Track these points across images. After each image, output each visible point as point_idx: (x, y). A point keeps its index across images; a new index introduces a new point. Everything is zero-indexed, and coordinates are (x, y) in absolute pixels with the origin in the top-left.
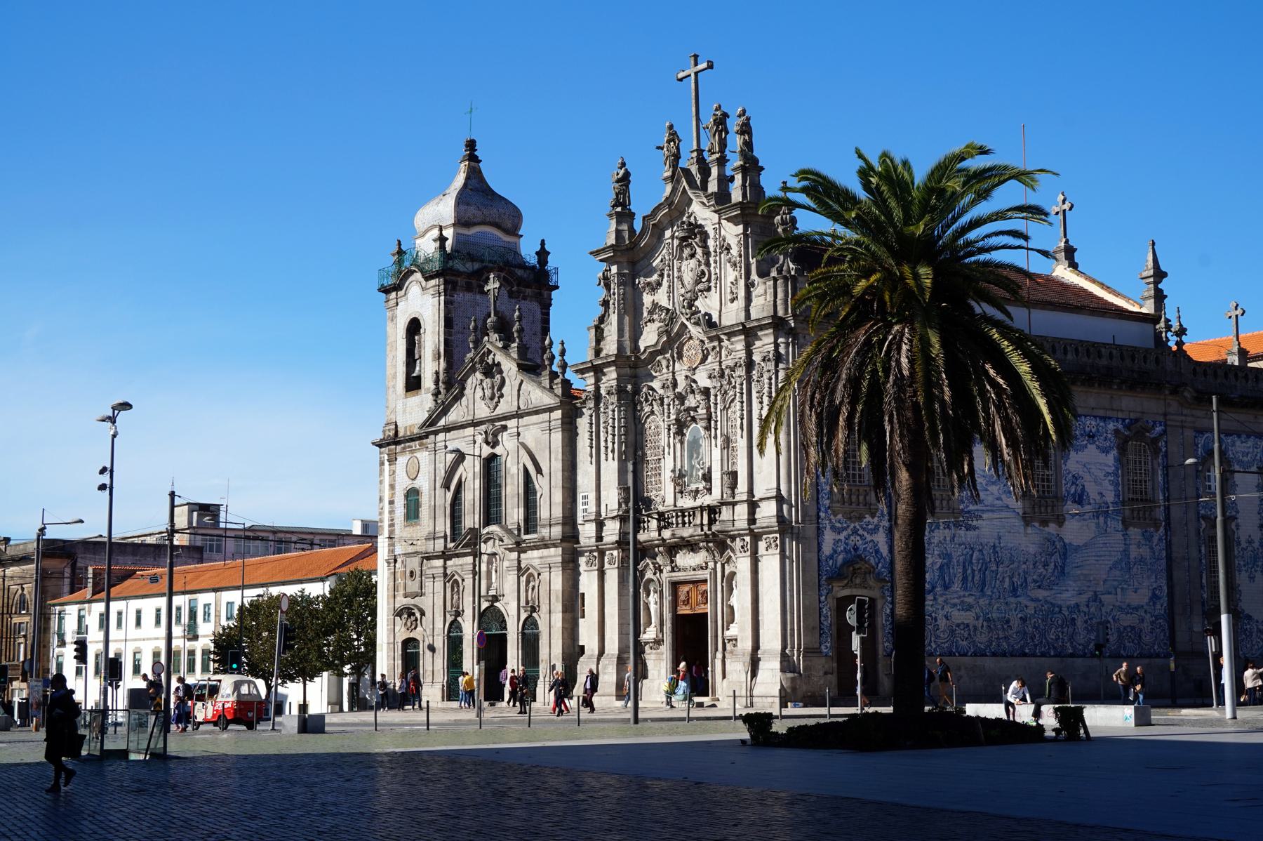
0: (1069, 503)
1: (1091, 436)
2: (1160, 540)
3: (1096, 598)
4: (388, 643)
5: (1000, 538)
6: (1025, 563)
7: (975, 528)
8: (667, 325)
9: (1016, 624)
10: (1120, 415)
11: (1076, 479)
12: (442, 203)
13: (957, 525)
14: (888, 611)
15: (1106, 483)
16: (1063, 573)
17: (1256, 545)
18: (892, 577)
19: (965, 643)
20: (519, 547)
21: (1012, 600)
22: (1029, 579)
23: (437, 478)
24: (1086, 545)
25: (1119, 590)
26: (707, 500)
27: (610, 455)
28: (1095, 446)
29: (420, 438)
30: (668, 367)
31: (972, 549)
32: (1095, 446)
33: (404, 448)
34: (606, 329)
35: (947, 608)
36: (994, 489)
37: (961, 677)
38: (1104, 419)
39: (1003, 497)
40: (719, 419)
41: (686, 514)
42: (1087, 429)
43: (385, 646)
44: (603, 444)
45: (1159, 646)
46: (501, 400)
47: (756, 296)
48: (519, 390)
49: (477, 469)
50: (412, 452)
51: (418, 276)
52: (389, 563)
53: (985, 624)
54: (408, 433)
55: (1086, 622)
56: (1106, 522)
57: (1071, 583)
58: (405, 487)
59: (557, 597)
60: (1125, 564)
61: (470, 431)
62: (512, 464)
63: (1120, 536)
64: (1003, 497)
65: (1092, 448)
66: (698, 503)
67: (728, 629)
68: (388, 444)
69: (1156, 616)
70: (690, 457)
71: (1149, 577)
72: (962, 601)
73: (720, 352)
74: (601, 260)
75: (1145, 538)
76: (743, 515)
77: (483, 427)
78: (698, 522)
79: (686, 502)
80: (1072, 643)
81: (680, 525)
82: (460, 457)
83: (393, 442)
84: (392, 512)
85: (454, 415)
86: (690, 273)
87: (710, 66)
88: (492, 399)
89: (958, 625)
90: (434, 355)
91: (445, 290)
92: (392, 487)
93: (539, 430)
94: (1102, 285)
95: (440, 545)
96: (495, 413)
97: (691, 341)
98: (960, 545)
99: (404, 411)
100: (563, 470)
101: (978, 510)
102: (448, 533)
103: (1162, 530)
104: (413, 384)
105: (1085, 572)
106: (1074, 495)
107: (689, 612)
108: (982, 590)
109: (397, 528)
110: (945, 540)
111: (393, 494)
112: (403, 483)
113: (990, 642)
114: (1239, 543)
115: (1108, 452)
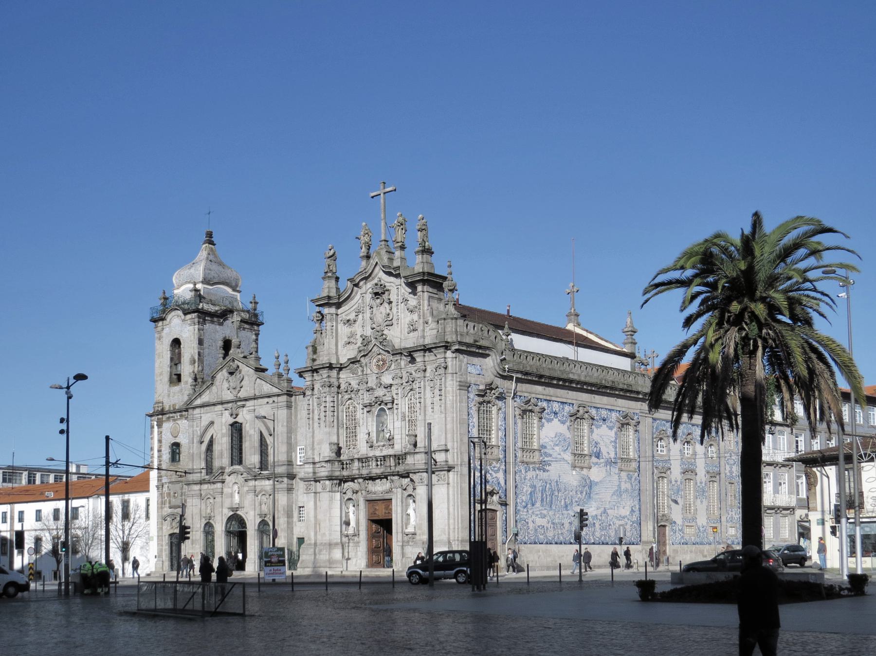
0: (593, 457)
1: (604, 420)
2: (635, 479)
3: (605, 512)
4: (158, 536)
5: (560, 477)
6: (572, 491)
7: (548, 471)
9: (567, 525)
10: (618, 409)
11: (597, 444)
12: (193, 268)
13: (539, 469)
14: (504, 518)
15: (611, 447)
16: (590, 497)
17: (679, 483)
18: (506, 498)
19: (542, 537)
20: (255, 478)
21: (565, 512)
22: (574, 501)
23: (195, 436)
24: (600, 482)
25: (616, 507)
26: (391, 452)
27: (323, 424)
28: (606, 426)
29: (180, 412)
30: (363, 371)
31: (546, 482)
32: (606, 426)
33: (169, 418)
34: (318, 348)
35: (534, 517)
36: (557, 448)
37: (540, 556)
38: (610, 410)
39: (562, 453)
40: (400, 404)
41: (379, 460)
42: (602, 416)
43: (155, 539)
44: (316, 417)
45: (634, 539)
46: (242, 389)
47: (430, 329)
49: (224, 431)
50: (174, 420)
51: (180, 313)
52: (158, 487)
53: (552, 526)
55: (600, 525)
56: (610, 469)
57: (594, 503)
59: (284, 509)
60: (619, 493)
61: (219, 407)
63: (617, 477)
64: (562, 453)
65: (604, 426)
67: (406, 528)
68: (158, 415)
69: (633, 522)
70: (377, 426)
71: (630, 500)
72: (541, 513)
73: (400, 363)
74: (317, 306)
75: (628, 478)
76: (421, 461)
77: (230, 405)
78: (388, 465)
79: (378, 453)
80: (593, 537)
82: (212, 423)
83: (161, 413)
84: (159, 457)
85: (205, 398)
87: (395, 190)
89: (539, 527)
90: (191, 361)
91: (199, 322)
92: (160, 441)
93: (270, 408)
94: (597, 336)
95: (196, 477)
97: (380, 357)
98: (540, 480)
100: (287, 433)
101: (548, 461)
103: (636, 474)
104: (177, 378)
105: (600, 497)
106: (596, 452)
108: (551, 507)
110: (533, 477)
112: (168, 440)
113: (555, 536)
114: (671, 483)
115: (612, 429)
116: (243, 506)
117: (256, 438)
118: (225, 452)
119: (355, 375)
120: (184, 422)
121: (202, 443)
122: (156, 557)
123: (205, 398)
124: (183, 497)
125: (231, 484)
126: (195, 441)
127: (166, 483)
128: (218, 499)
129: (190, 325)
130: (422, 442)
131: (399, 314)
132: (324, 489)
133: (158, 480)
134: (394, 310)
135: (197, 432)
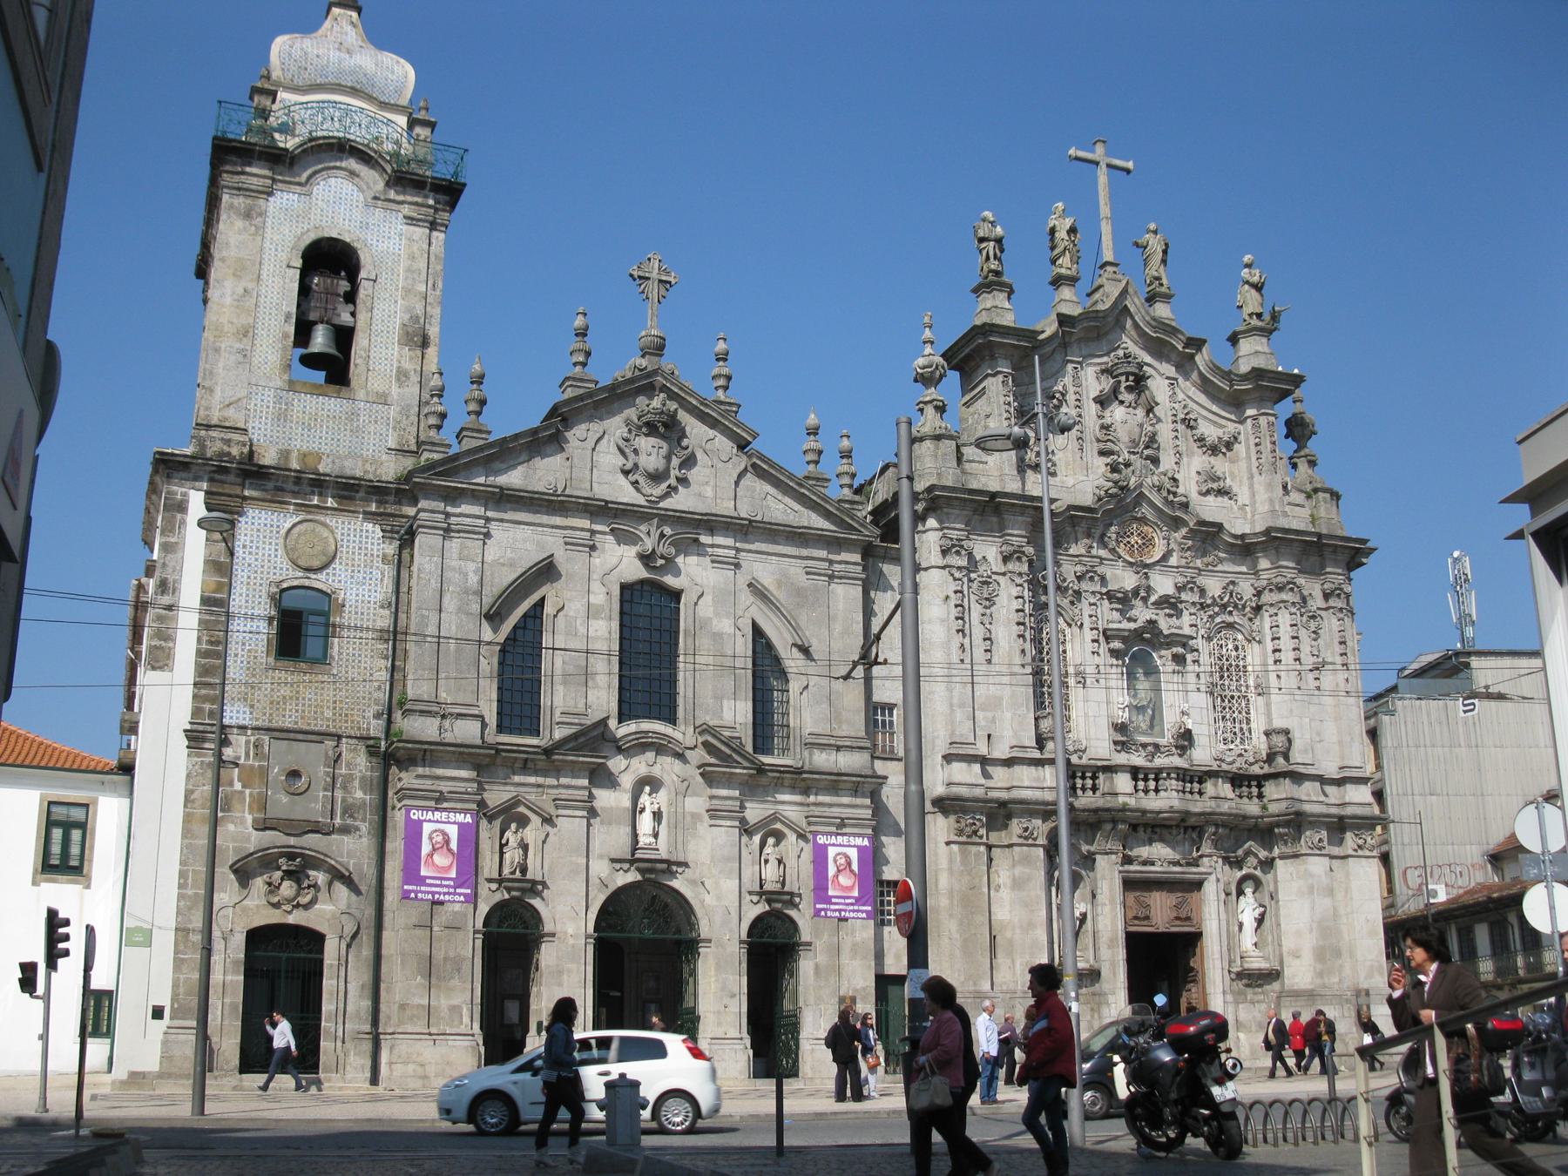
4: (182, 931)
8: (1122, 488)
44: (978, 632)
47: (1289, 504)
48: (737, 483)
49: (598, 598)
52: (195, 738)
54: (295, 465)
62: (717, 614)
66: (1160, 761)
87: (1128, 171)
88: (656, 477)
93: (801, 571)
95: (466, 731)
96: (661, 505)
99: (282, 417)
102: (489, 709)
122: (158, 1013)
124: (339, 794)
125: (627, 781)
126: (450, 603)
127: (243, 728)
129: (410, 220)
130: (1306, 751)
132: (1026, 838)
133: (196, 712)
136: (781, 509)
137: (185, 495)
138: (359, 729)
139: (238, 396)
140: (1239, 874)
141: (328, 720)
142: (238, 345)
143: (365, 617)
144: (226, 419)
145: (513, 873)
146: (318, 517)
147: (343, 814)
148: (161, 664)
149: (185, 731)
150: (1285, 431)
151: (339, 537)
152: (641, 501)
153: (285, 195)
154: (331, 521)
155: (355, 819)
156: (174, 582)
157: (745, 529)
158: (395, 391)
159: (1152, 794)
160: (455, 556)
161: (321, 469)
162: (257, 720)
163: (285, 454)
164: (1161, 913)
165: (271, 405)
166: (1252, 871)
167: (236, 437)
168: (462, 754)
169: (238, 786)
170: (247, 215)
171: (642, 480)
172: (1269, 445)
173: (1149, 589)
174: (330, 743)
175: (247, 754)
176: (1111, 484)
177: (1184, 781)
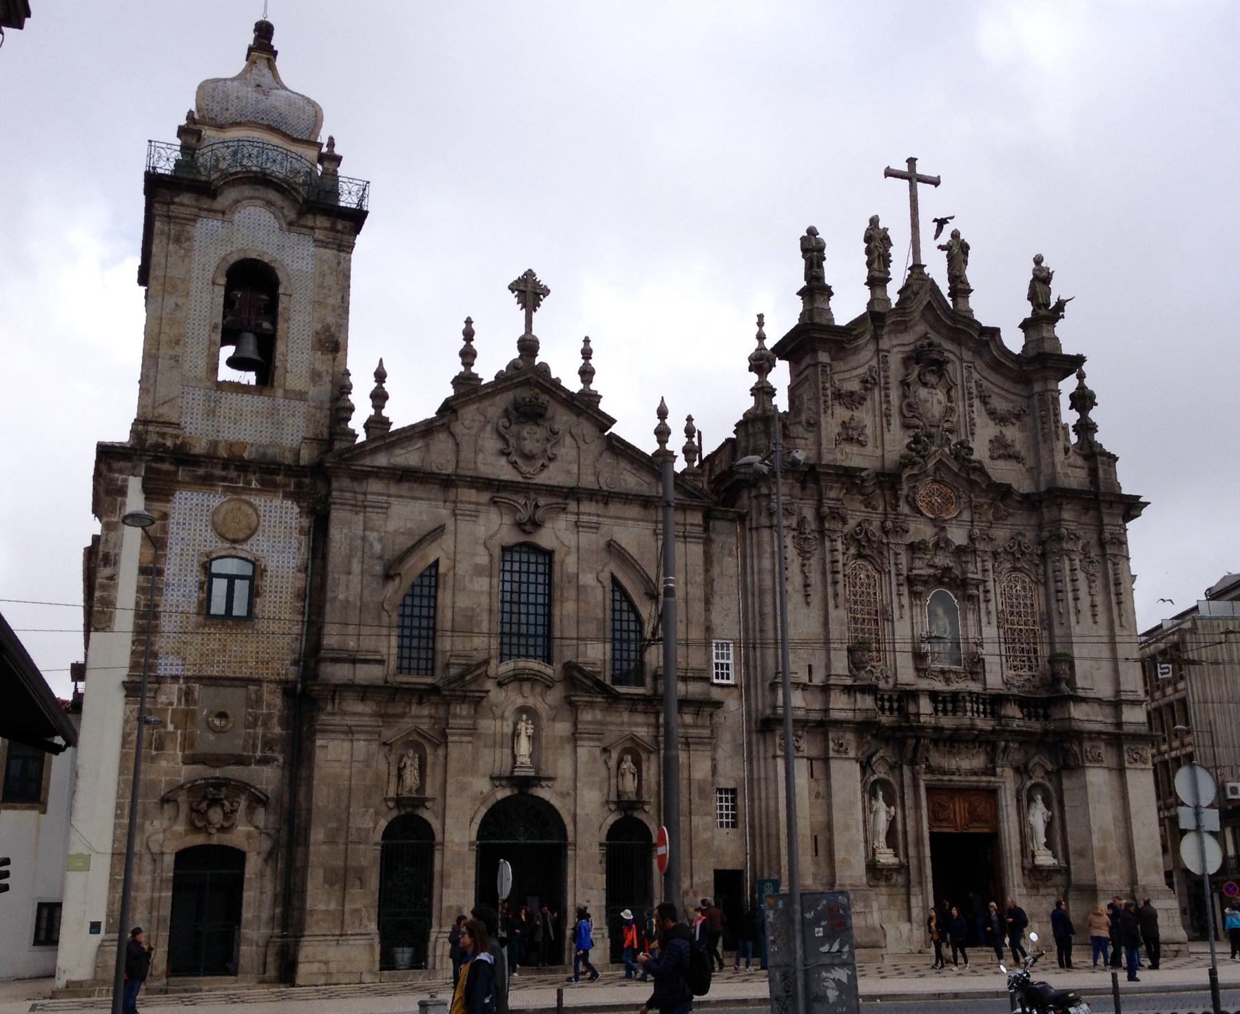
46: (552, 466)
49: (483, 559)
50: (235, 491)
54: (223, 453)
58: (203, 549)
81: (976, 715)
82: (438, 531)
86: (936, 406)
88: (529, 457)
93: (649, 532)
95: (367, 674)
97: (936, 486)
99: (211, 413)
107: (953, 831)
109: (168, 624)
111: (156, 558)
116: (550, 773)
117: (600, 598)
118: (485, 616)
119: (870, 510)
120: (277, 502)
121: (388, 577)
123: (408, 457)
124: (260, 730)
126: (356, 567)
127: (175, 678)
128: (458, 750)
129: (319, 243)
131: (975, 416)
133: (134, 666)
134: (960, 408)
135: (364, 538)
136: (632, 481)
137: (125, 480)
138: (278, 675)
139: (172, 396)
140: (1029, 784)
141: (251, 668)
142: (171, 352)
143: (285, 580)
144: (161, 415)
145: (411, 790)
146: (244, 497)
147: (263, 747)
148: (104, 626)
149: (123, 682)
150: (1069, 402)
151: (262, 513)
152: (520, 479)
153: (211, 223)
154: (256, 500)
155: (273, 751)
156: (116, 555)
157: (603, 497)
158: (312, 391)
159: (950, 713)
160: (361, 527)
161: (246, 455)
162: (188, 670)
163: (214, 444)
164: (959, 815)
165: (201, 402)
166: (1040, 780)
167: (169, 430)
168: (364, 691)
169: (170, 727)
170: (178, 240)
171: (519, 461)
172: (1052, 417)
173: (948, 542)
174: (252, 688)
175: (179, 700)
176: (914, 454)
177: (977, 703)
